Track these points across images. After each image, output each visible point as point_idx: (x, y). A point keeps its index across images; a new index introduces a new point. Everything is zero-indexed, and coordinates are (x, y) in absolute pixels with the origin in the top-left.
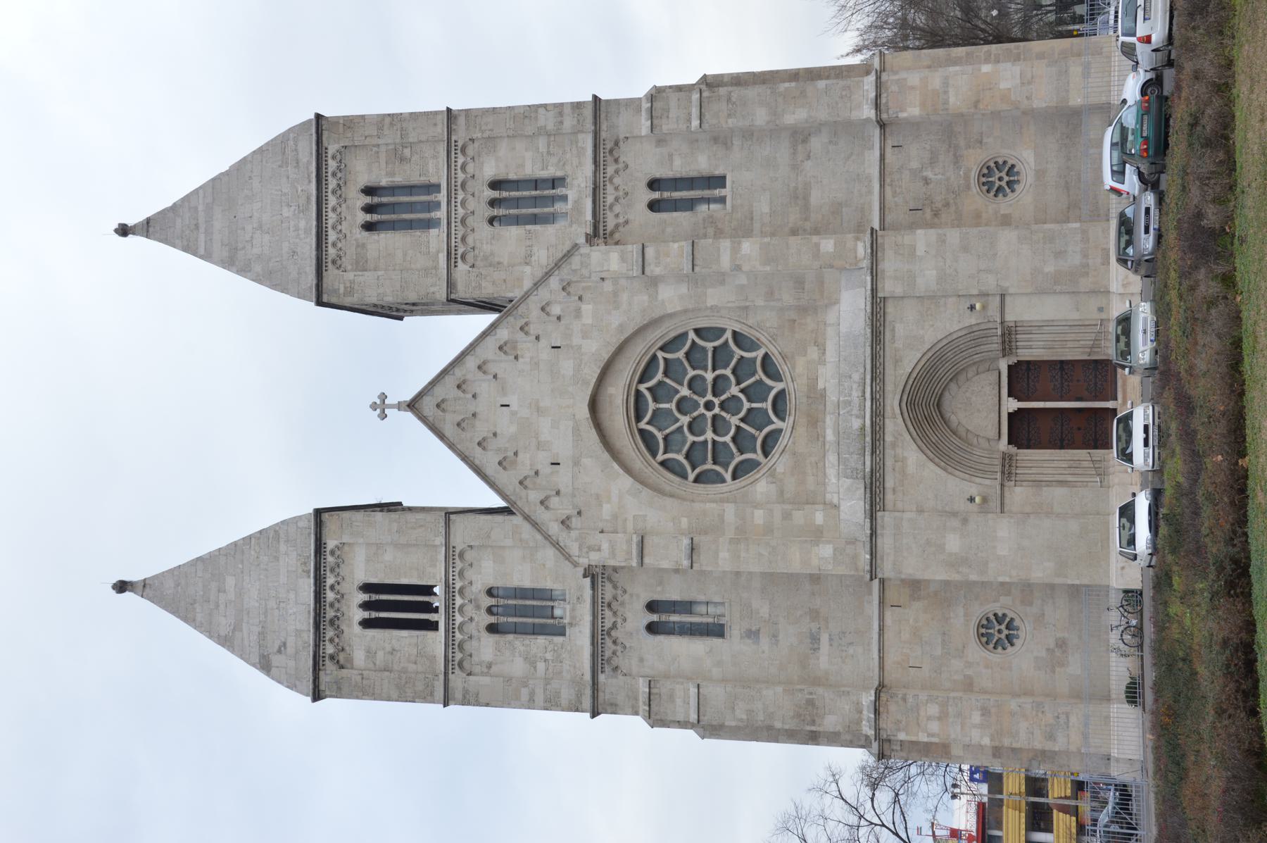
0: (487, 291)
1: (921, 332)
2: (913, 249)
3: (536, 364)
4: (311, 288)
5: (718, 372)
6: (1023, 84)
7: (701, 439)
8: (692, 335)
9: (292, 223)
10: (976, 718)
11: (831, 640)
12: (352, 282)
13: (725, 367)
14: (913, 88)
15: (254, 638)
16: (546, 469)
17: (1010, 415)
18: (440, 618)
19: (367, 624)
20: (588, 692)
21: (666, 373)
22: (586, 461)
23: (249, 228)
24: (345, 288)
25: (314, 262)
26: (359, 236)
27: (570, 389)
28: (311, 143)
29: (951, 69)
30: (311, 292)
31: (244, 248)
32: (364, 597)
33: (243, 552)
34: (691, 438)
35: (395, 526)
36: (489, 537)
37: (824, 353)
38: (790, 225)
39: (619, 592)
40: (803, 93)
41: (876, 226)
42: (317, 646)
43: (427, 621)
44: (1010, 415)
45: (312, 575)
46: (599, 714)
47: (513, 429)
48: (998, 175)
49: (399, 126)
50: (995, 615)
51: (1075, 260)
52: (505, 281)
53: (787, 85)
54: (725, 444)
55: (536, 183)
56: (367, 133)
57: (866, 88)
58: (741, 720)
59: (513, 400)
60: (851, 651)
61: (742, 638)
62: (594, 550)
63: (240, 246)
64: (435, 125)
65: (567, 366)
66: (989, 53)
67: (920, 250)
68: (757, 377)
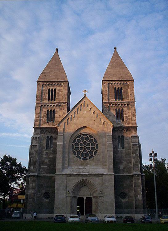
3: (92, 117)
5: (91, 148)
7: (79, 145)
19: (49, 89)
21: (90, 139)
29: (141, 187)
35: (65, 94)
36: (63, 110)
44: (83, 198)
50: (50, 195)
54: (78, 149)
55: (123, 116)
65: (91, 122)
68: (85, 156)
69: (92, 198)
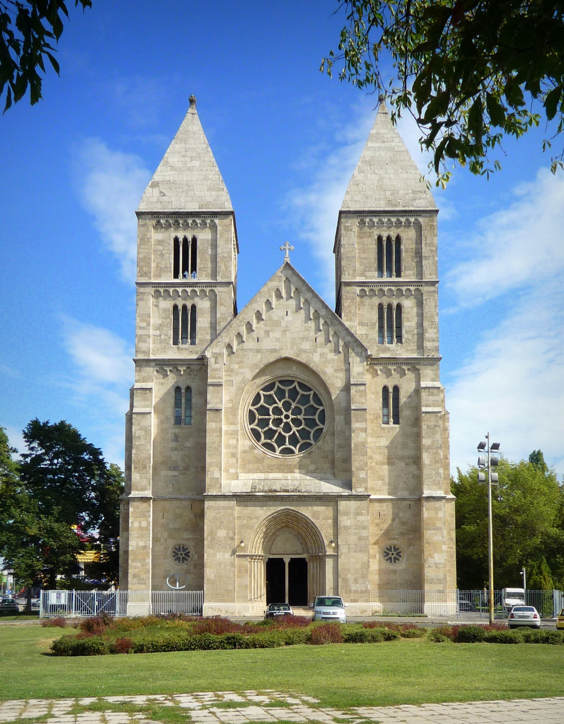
0: (345, 303)
1: (321, 518)
2: (361, 514)
4: (349, 207)
5: (303, 421)
6: (436, 564)
7: (271, 413)
8: (321, 408)
9: (382, 196)
10: (142, 544)
11: (175, 476)
12: (351, 230)
13: (306, 425)
14: (437, 514)
15: (167, 178)
16: (254, 335)
17: (283, 559)
18: (180, 279)
19: (176, 240)
20: (146, 358)
22: (259, 356)
23: (381, 172)
24: (348, 226)
25: (362, 209)
26: (375, 233)
27: (295, 347)
28: (423, 207)
30: (347, 208)
31: (370, 169)
32: (190, 239)
33: (211, 170)
34: (271, 408)
36: (221, 305)
37: (312, 472)
38: (374, 456)
39: (195, 373)
40: (437, 462)
41: (371, 497)
42: (164, 213)
43: (178, 272)
44: (283, 559)
45: (201, 210)
46: (135, 363)
47: (275, 318)
48: (395, 553)
49: (431, 255)
51: (353, 587)
52: (350, 312)
53: (442, 454)
55: (399, 327)
56: (428, 238)
57: (438, 492)
58: (135, 433)
59: (290, 317)
60: (170, 485)
61: (175, 433)
62: (216, 360)
63: (372, 167)
64: (431, 274)
65: (306, 346)
66: (452, 548)
67: (360, 518)
69: (307, 560)
